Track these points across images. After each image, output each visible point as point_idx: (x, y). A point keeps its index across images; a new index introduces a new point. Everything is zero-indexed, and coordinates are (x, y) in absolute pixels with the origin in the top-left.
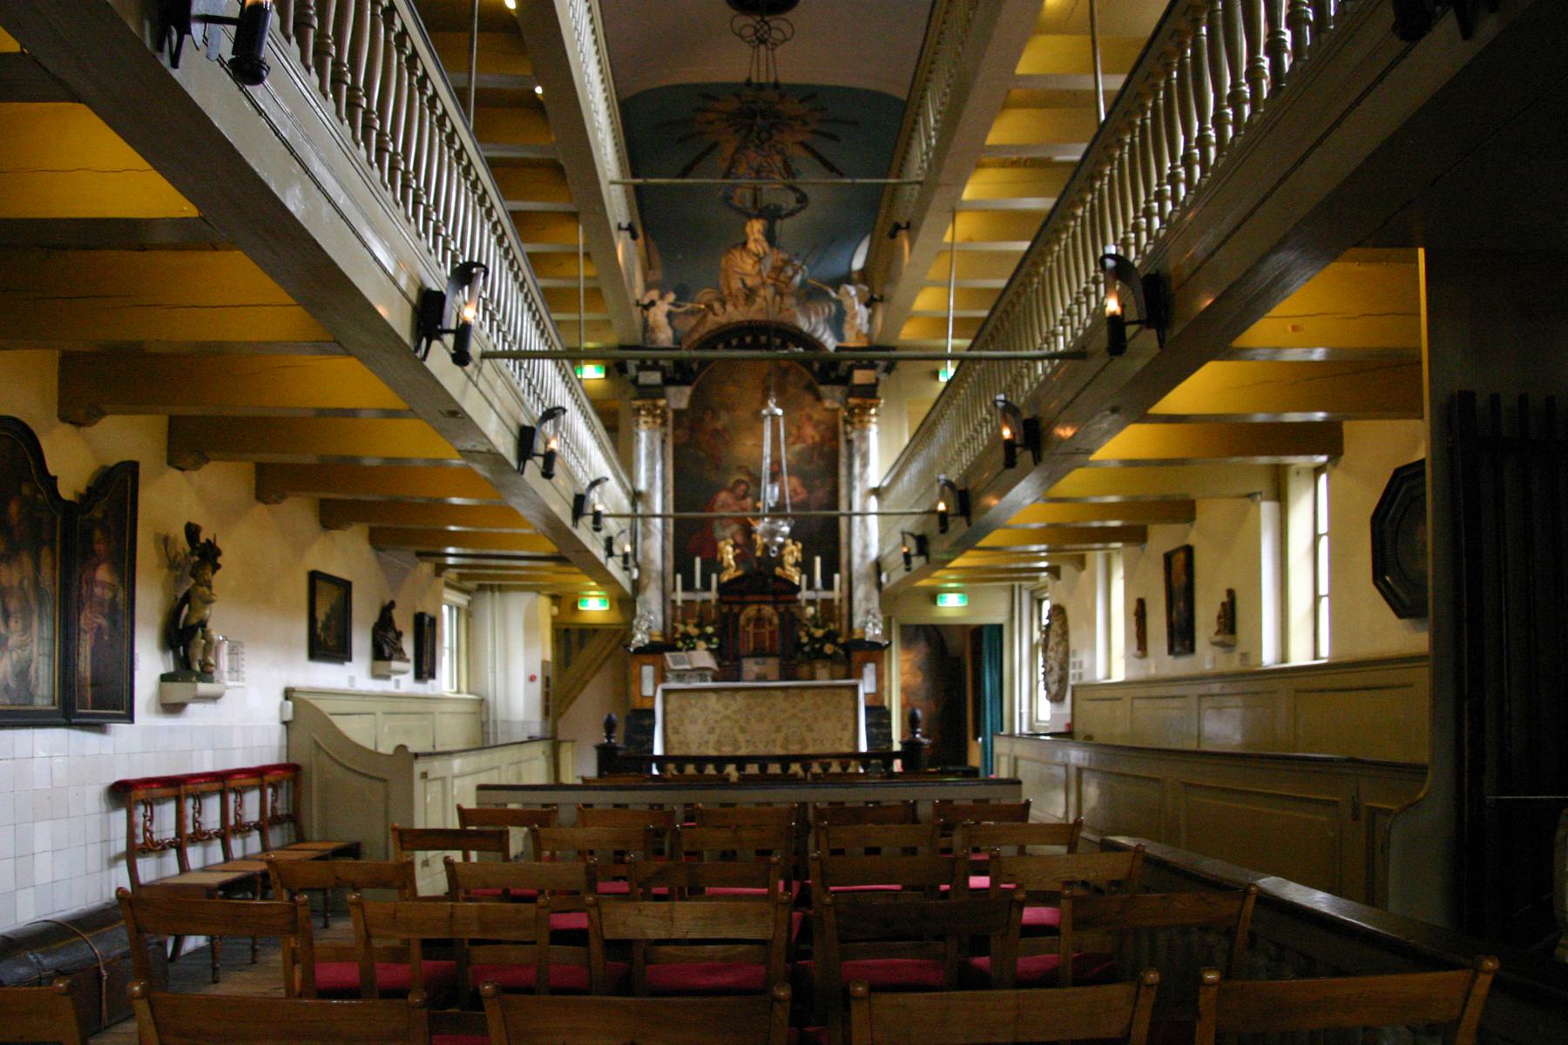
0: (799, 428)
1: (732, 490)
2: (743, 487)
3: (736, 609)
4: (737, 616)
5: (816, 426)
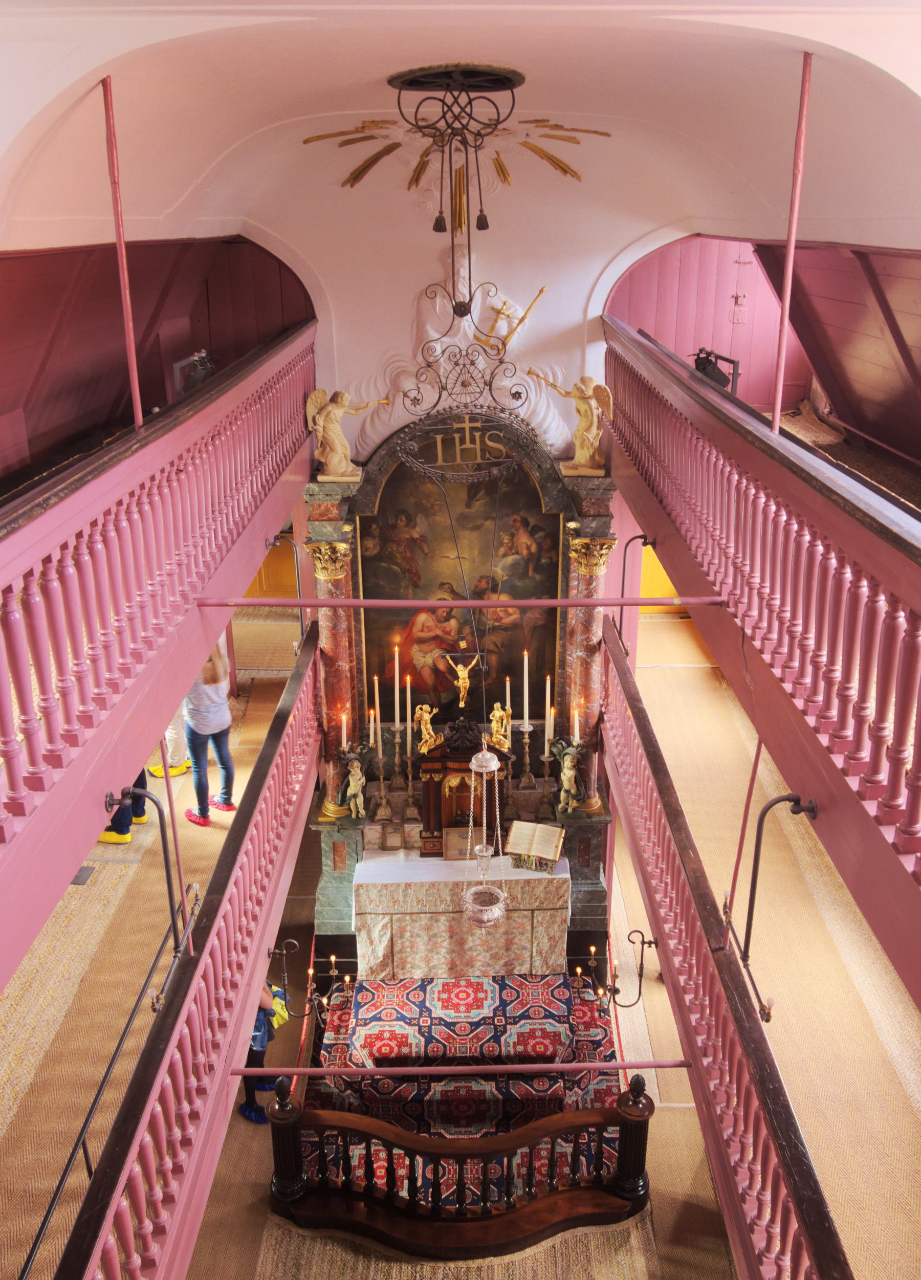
0: (512, 536)
4: (440, 784)
5: (532, 533)
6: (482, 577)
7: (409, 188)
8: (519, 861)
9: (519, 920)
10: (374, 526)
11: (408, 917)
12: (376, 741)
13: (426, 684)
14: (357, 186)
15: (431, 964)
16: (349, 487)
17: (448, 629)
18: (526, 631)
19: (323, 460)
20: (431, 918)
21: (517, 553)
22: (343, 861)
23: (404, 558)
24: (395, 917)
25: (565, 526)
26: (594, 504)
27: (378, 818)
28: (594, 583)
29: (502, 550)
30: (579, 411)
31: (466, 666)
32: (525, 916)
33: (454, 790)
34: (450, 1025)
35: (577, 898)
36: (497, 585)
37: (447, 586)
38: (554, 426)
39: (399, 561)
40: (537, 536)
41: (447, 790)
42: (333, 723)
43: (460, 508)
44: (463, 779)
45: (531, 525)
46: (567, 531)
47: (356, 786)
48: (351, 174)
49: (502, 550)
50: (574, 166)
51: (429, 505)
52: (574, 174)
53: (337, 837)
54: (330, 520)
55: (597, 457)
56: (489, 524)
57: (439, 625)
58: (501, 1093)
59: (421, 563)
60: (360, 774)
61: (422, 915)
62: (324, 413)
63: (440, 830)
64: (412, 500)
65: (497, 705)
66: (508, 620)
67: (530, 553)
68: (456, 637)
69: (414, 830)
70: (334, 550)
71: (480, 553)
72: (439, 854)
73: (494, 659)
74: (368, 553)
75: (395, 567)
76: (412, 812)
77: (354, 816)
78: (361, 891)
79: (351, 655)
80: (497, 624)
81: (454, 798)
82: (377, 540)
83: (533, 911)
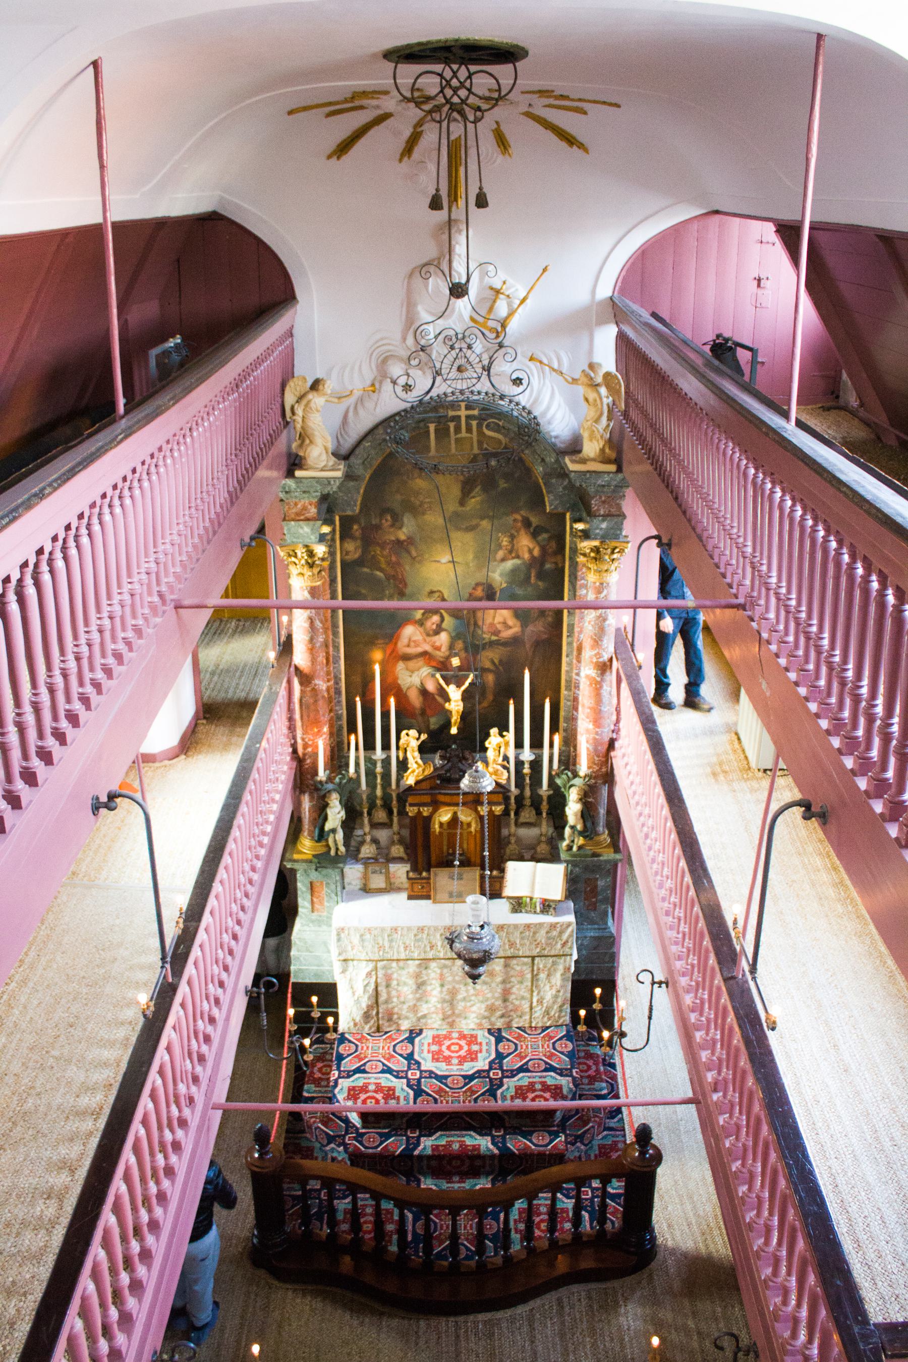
0: (512, 537)
1: (421, 623)
2: (436, 618)
3: (426, 811)
4: (429, 819)
5: (534, 535)
6: (477, 584)
7: (400, 160)
8: (518, 905)
9: (518, 968)
10: (355, 527)
11: (394, 964)
12: (357, 771)
13: (414, 708)
14: (344, 158)
15: (420, 1015)
16: (329, 483)
17: (438, 644)
18: (528, 646)
19: (301, 454)
20: (420, 965)
21: (518, 557)
22: (321, 903)
23: (389, 563)
24: (380, 964)
25: (571, 528)
26: (604, 502)
27: (361, 856)
28: (605, 592)
29: (500, 554)
30: (587, 400)
31: (459, 686)
32: (525, 964)
33: (445, 827)
34: (442, 1078)
35: (582, 945)
36: (495, 593)
37: (437, 595)
38: (559, 416)
39: (383, 566)
40: (540, 538)
41: (437, 826)
42: (310, 749)
43: (452, 506)
44: (455, 813)
45: (534, 525)
46: (574, 534)
47: (334, 820)
48: (339, 146)
49: (500, 554)
50: (581, 138)
51: (418, 503)
52: (581, 146)
53: (314, 875)
54: (308, 519)
55: (607, 450)
56: (485, 524)
57: (428, 639)
58: (498, 1148)
59: (407, 568)
60: (339, 807)
61: (410, 962)
62: (304, 402)
63: (428, 871)
64: (399, 497)
65: (494, 731)
66: (506, 634)
67: (533, 558)
68: (447, 653)
69: (400, 871)
70: (311, 554)
71: (476, 557)
72: (428, 897)
73: (490, 678)
74: (348, 558)
75: (378, 573)
76: (398, 850)
77: (333, 853)
78: (342, 935)
79: (328, 673)
80: (494, 638)
81: (445, 834)
82: (359, 543)
83: (533, 958)
